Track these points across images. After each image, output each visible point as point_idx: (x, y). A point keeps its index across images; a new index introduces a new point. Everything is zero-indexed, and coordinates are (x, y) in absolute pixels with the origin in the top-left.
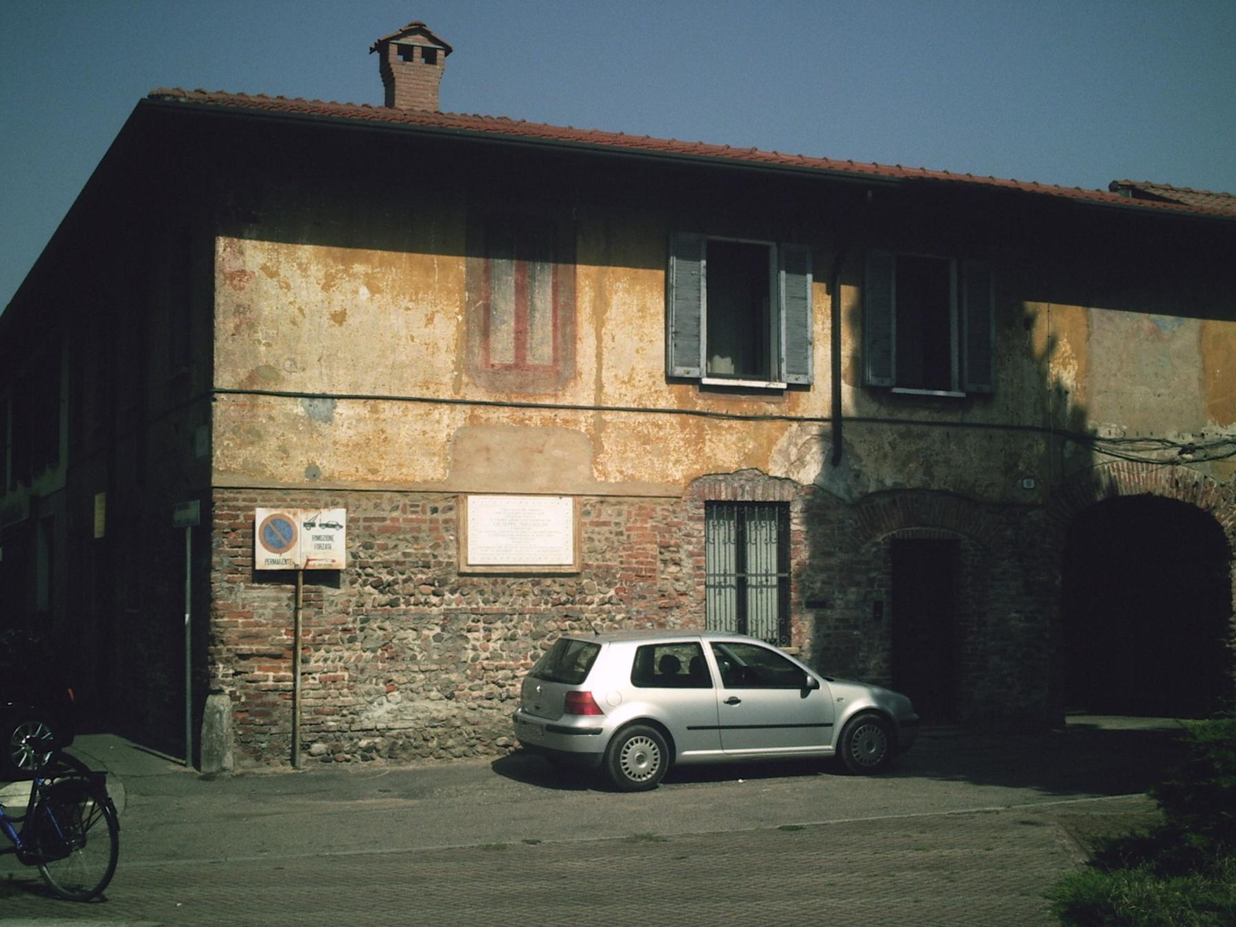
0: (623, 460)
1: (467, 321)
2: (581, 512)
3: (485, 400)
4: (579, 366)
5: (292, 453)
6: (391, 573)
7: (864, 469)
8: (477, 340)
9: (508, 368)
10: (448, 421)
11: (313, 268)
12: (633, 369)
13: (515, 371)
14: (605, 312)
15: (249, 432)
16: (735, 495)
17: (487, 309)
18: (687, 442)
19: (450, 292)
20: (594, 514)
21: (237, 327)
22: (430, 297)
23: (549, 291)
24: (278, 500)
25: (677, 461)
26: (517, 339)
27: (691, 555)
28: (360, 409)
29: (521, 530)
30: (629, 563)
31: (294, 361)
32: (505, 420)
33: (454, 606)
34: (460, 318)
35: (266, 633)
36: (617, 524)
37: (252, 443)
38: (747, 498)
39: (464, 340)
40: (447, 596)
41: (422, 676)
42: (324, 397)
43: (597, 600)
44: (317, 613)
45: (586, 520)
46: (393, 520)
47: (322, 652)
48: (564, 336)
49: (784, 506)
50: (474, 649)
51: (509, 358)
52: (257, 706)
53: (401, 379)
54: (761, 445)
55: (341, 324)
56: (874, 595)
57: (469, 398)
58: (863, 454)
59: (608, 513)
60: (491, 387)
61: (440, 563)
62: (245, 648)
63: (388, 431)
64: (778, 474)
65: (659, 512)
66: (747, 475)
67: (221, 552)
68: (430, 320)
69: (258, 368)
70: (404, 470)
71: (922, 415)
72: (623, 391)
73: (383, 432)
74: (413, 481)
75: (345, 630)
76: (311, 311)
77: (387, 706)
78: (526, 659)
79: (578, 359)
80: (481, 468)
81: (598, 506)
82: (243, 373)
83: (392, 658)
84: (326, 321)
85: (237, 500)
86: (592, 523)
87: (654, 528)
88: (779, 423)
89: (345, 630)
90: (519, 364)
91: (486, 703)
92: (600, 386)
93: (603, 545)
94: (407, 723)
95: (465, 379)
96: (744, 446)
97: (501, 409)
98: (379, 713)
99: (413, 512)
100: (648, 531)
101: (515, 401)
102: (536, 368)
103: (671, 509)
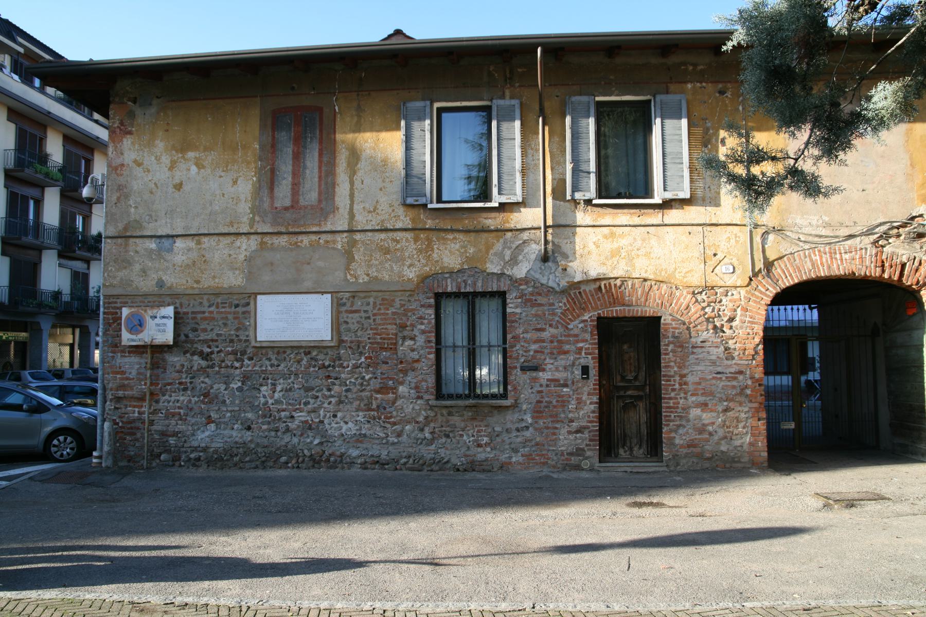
0: (369, 266)
1: (259, 181)
2: (338, 306)
3: (271, 231)
4: (337, 203)
5: (149, 273)
6: (209, 347)
8: (266, 192)
9: (286, 209)
10: (247, 246)
12: (377, 202)
13: (291, 211)
14: (357, 164)
15: (123, 261)
16: (460, 288)
17: (273, 171)
18: (420, 251)
19: (248, 163)
20: (348, 304)
21: (118, 199)
22: (236, 167)
23: (316, 154)
26: (293, 189)
27: (423, 332)
28: (191, 243)
29: (293, 318)
30: (375, 339)
31: (151, 216)
33: (250, 368)
36: (365, 311)
37: (125, 268)
39: (257, 191)
40: (246, 361)
41: (229, 414)
44: (163, 373)
45: (343, 309)
47: (167, 397)
48: (326, 184)
49: (502, 295)
50: (264, 397)
51: (288, 203)
53: (215, 222)
54: (480, 250)
55: (179, 190)
56: (582, 361)
57: (259, 231)
60: (275, 223)
61: (240, 341)
62: (121, 393)
64: (495, 271)
65: (397, 303)
68: (235, 182)
70: (217, 280)
72: (370, 218)
75: (180, 383)
77: (207, 433)
79: (336, 199)
80: (266, 277)
82: (121, 226)
84: (171, 189)
85: (116, 303)
86: (347, 311)
87: (394, 313)
90: (294, 205)
91: (273, 434)
92: (352, 215)
93: (355, 327)
94: (218, 444)
95: (257, 218)
98: (203, 436)
99: (223, 307)
100: (390, 316)
102: (306, 207)
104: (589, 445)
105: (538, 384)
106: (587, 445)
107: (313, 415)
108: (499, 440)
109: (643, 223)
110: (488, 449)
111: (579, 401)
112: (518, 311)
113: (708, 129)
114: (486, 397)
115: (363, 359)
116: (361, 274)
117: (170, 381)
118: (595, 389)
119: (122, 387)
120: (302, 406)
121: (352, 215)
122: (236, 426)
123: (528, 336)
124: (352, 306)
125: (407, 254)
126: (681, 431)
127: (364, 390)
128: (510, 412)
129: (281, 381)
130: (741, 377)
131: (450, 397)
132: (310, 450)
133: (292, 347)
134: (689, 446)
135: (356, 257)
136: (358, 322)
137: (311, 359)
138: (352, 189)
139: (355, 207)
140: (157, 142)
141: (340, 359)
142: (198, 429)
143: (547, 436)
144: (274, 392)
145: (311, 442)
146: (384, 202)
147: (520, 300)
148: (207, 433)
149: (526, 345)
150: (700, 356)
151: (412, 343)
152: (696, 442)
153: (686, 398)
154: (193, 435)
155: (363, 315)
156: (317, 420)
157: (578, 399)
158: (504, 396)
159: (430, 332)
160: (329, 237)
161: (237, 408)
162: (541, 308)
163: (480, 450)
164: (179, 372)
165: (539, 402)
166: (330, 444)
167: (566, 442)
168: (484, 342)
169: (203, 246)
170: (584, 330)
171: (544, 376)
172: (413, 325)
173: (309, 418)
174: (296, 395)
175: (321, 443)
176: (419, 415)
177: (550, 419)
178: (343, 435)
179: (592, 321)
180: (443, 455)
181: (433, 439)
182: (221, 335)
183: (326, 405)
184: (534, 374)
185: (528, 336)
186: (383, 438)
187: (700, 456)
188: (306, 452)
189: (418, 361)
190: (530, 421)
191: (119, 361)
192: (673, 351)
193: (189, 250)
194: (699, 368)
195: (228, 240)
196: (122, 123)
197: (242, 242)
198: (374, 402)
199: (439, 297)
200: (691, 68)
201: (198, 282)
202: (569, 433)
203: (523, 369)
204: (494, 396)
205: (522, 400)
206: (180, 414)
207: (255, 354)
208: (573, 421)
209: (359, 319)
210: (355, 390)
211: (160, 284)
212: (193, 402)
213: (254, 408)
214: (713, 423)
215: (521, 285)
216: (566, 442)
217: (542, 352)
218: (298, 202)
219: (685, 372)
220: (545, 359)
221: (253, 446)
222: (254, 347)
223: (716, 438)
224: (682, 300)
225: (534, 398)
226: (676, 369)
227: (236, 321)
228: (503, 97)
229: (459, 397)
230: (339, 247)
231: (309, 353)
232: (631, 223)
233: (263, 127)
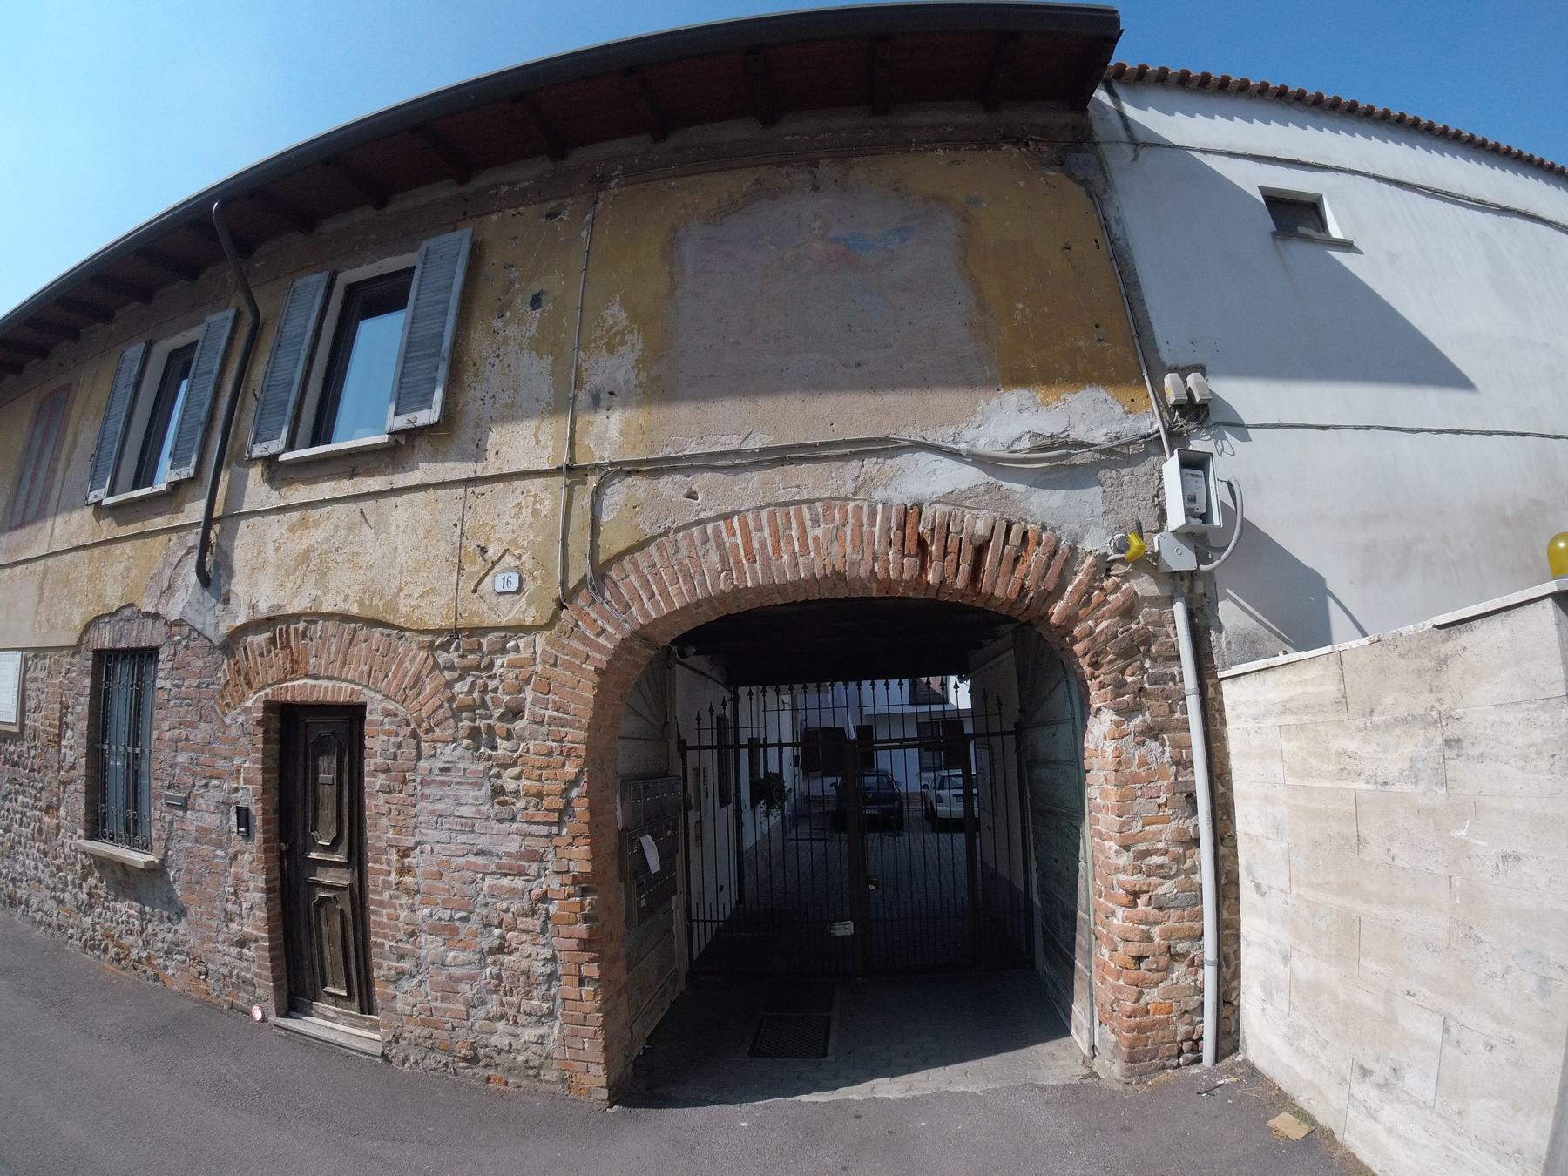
113: (512, 283)
126: (406, 984)
130: (533, 868)
150: (439, 806)
214: (472, 979)
226: (391, 834)
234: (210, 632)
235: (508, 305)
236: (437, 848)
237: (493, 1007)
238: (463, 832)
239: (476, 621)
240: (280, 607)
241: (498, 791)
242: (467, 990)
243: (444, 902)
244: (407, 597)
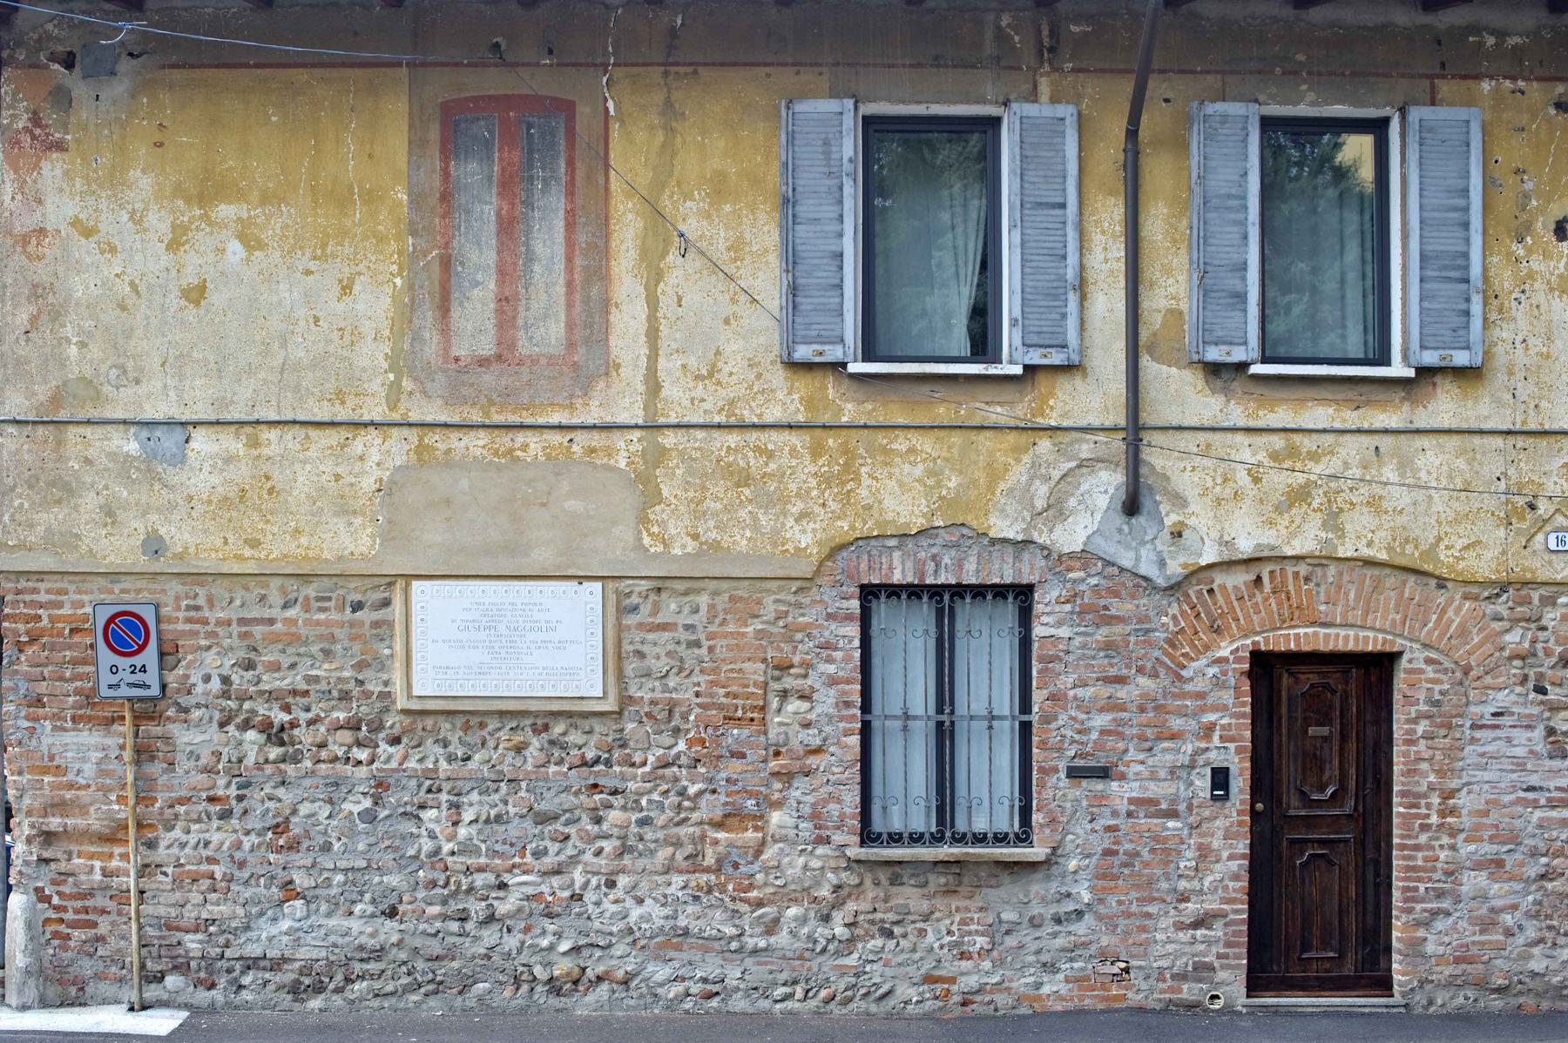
0: (700, 515)
2: (621, 608)
3: (443, 418)
4: (614, 351)
6: (287, 708)
7: (1191, 522)
9: (483, 362)
10: (379, 456)
11: (152, 218)
12: (718, 353)
13: (496, 367)
15: (52, 484)
16: (923, 575)
17: (446, 263)
18: (826, 481)
19: (381, 239)
20: (646, 609)
21: (34, 319)
23: (560, 224)
24: (101, 591)
25: (803, 516)
26: (500, 312)
27: (833, 681)
28: (232, 443)
29: (503, 638)
30: (712, 695)
32: (478, 452)
33: (394, 764)
34: (398, 281)
35: (87, 800)
36: (688, 627)
37: (59, 502)
38: (946, 578)
39: (406, 313)
41: (340, 878)
42: (170, 423)
43: (651, 759)
44: (165, 771)
45: (631, 620)
46: (288, 621)
47: (177, 833)
48: (587, 300)
49: (1023, 593)
50: (432, 836)
51: (487, 347)
52: (77, 912)
54: (974, 482)
55: (197, 303)
56: (1212, 755)
57: (414, 417)
58: (1191, 493)
59: (671, 608)
60: (453, 398)
62: (54, 823)
63: (276, 475)
64: (1011, 535)
65: (769, 608)
66: (944, 536)
67: (16, 672)
68: (346, 289)
69: (65, 384)
70: (304, 540)
71: (1319, 414)
72: (699, 392)
73: (268, 478)
74: (317, 559)
75: (211, 800)
76: (149, 287)
77: (285, 925)
78: (523, 856)
79: (614, 341)
80: (433, 534)
81: (653, 597)
82: (43, 392)
83: (290, 848)
84: (174, 301)
85: (35, 591)
86: (640, 626)
88: (1011, 438)
89: (211, 800)
90: (504, 355)
91: (454, 926)
92: (654, 386)
93: (662, 665)
95: (407, 384)
96: (939, 484)
97: (472, 433)
98: (273, 933)
101: (498, 418)
102: (534, 361)
103: (792, 598)
104: (1226, 956)
105: (1107, 811)
106: (1219, 956)
107: (556, 881)
108: (1011, 941)
109: (1366, 426)
110: (987, 965)
111: (1204, 853)
112: (1064, 632)
113: (1526, 196)
114: (980, 839)
115: (682, 746)
116: (676, 538)
117: (184, 793)
118: (1240, 823)
119: (60, 807)
120: (529, 859)
121: (654, 386)
122: (358, 908)
123: (1086, 693)
124: (654, 613)
125: (793, 487)
126: (1440, 925)
127: (686, 819)
128: (1039, 876)
129: (475, 796)
131: (895, 839)
132: (548, 965)
133: (502, 714)
134: (1457, 961)
135: (665, 493)
136: (669, 654)
137: (552, 743)
138: (652, 319)
139: (662, 363)
140: (134, 174)
141: (623, 746)
142: (262, 914)
143: (1127, 933)
144: (455, 824)
145: (551, 948)
146: (735, 350)
147: (1068, 607)
148: (285, 925)
149: (1084, 716)
150: (1489, 748)
151: (806, 705)
152: (1474, 950)
153: (1453, 848)
154: (247, 928)
155: (684, 636)
156: (567, 894)
157: (1200, 847)
158: (1024, 838)
159: (848, 682)
160: (596, 439)
161: (364, 864)
162: (1119, 629)
163: (966, 965)
164: (208, 770)
165: (1108, 853)
166: (598, 953)
167: (1170, 948)
168: (979, 707)
169: (266, 451)
170: (1218, 683)
171: (1120, 792)
172: (807, 665)
173: (545, 889)
174: (514, 830)
175: (576, 950)
176: (817, 884)
177: (1134, 894)
178: (631, 931)
179: (1238, 660)
180: (877, 980)
181: (852, 940)
182: (316, 679)
183: (588, 857)
184: (1099, 786)
185: (1086, 693)
186: (732, 938)
187: (1481, 984)
188: (538, 970)
189: (818, 751)
190: (1086, 897)
191: (46, 741)
192: (1428, 737)
193: (228, 460)
194: (1487, 776)
195: (332, 437)
196: (36, 120)
197: (369, 444)
198: (709, 852)
199: (869, 593)
200: (1491, 41)
201: (254, 544)
202: (1180, 926)
203: (1074, 773)
204: (1001, 839)
205: (1069, 847)
206: (212, 877)
207: (408, 731)
208: (1187, 900)
209: (671, 647)
210: (661, 820)
211: (154, 545)
212: (247, 846)
213: (402, 862)
214: (1515, 907)
215: (1069, 570)
216: (1170, 948)
217: (1121, 736)
218: (512, 346)
219: (1454, 784)
220: (1126, 751)
221: (403, 956)
222: (406, 712)
223: (1520, 940)
224: (1450, 613)
225: (1100, 843)
226: (1432, 778)
227: (357, 647)
228: (1033, 97)
229: (916, 839)
230: (622, 464)
231: (546, 728)
232: (1337, 425)
233: (417, 145)
234: (1147, 568)
235: (1528, 228)
236: (1486, 787)
237: (1531, 933)
238: (1513, 771)
239: (1529, 576)
240: (1273, 548)
241: (1551, 731)
242: (1508, 919)
243: (1491, 838)
244: (1447, 548)
